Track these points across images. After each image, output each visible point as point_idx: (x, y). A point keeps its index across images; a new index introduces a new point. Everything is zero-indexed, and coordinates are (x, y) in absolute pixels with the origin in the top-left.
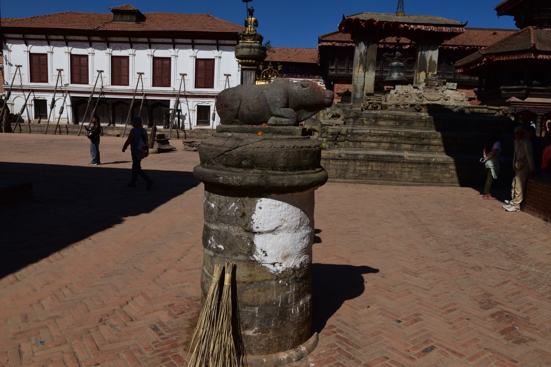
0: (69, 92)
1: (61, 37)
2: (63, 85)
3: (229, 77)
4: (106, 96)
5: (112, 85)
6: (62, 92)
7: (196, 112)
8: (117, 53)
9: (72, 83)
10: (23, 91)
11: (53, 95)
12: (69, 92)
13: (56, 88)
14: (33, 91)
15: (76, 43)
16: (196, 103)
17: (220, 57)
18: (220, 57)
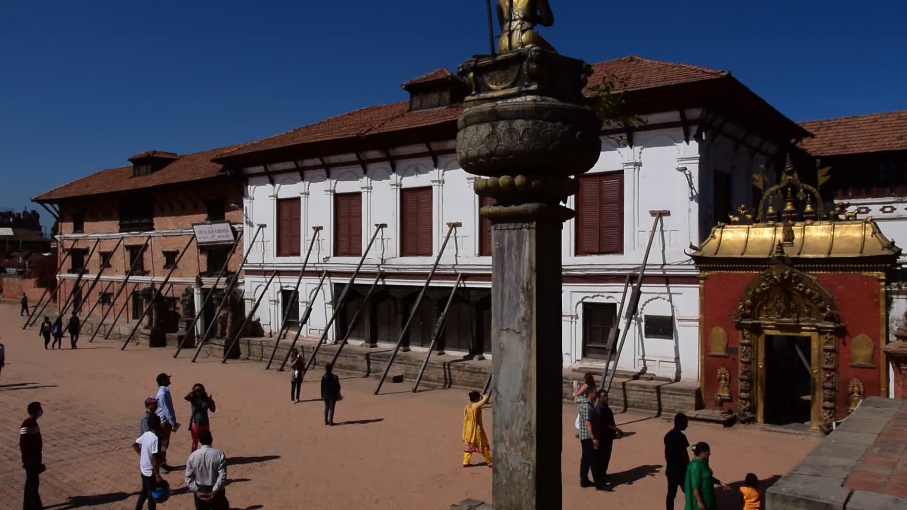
0: (330, 274)
1: (352, 157)
2: (321, 261)
3: (664, 218)
4: (389, 282)
5: (402, 255)
6: (318, 274)
7: (580, 321)
8: (411, 182)
9: (336, 254)
10: (265, 273)
11: (297, 280)
12: (330, 274)
13: (305, 267)
14: (278, 273)
15: (343, 170)
16: (579, 297)
17: (638, 165)
18: (638, 165)
